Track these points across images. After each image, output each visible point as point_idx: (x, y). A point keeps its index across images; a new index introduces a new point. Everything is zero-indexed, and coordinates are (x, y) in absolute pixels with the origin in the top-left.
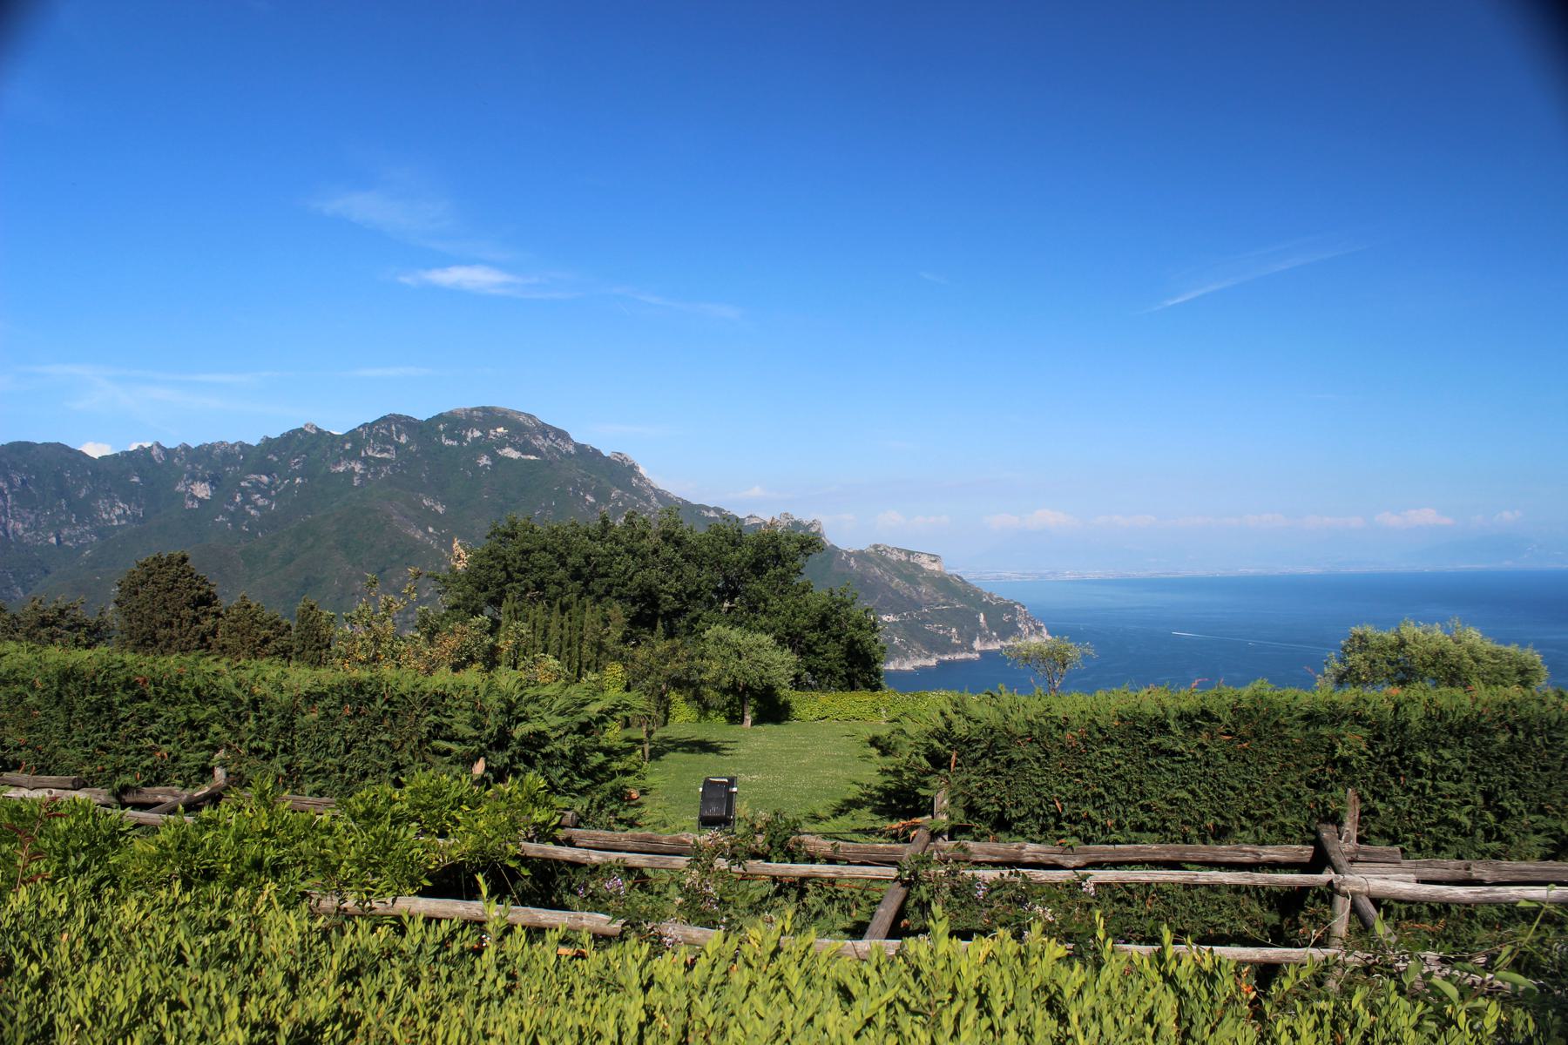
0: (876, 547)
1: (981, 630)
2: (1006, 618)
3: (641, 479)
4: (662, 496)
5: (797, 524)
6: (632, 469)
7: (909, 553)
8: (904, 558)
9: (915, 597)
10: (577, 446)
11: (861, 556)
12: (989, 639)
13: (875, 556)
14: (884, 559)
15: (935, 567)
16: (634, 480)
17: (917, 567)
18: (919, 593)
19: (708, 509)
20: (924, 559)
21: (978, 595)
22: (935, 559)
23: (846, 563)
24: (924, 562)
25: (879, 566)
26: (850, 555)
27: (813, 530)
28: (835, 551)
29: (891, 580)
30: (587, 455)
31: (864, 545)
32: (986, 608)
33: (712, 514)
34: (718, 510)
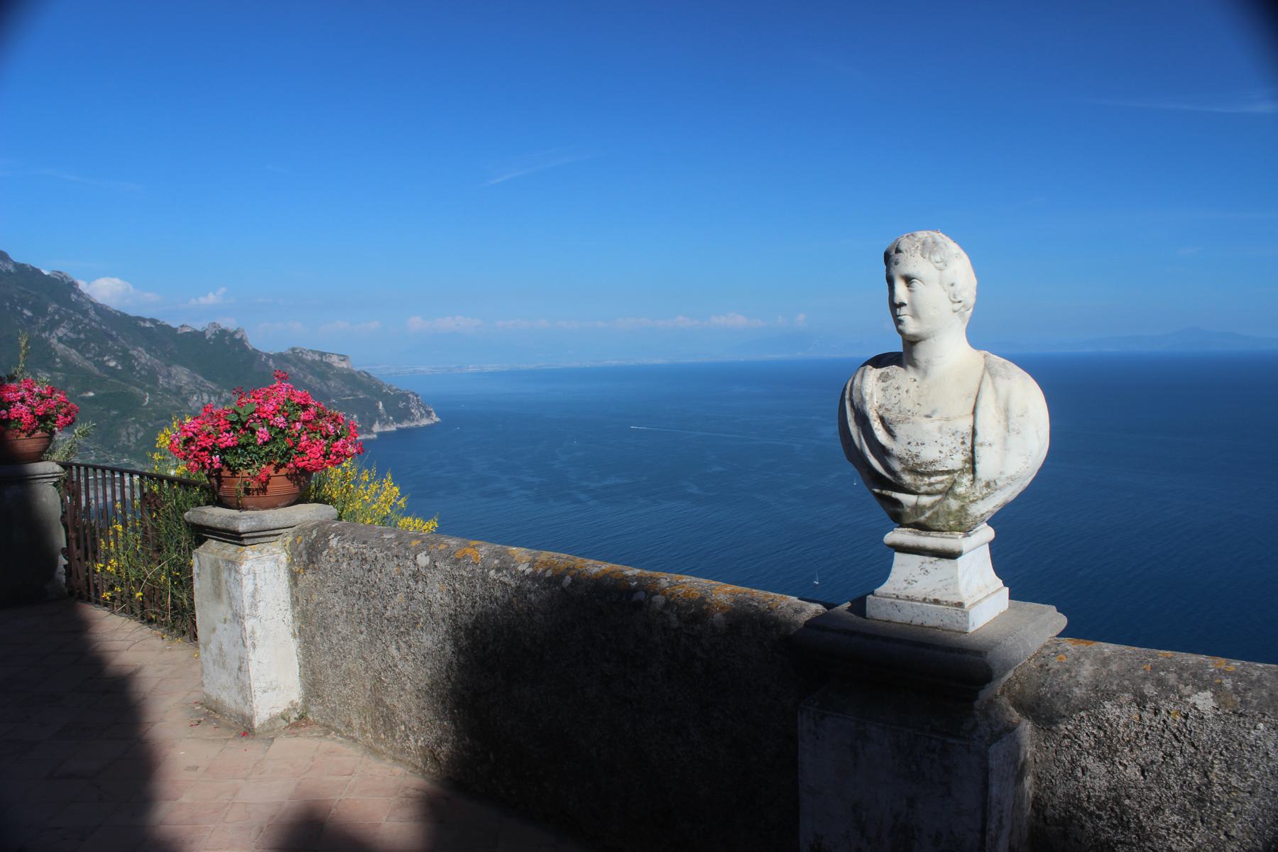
0: (293, 349)
1: (379, 416)
2: (401, 405)
3: (80, 294)
4: (101, 310)
5: (224, 332)
6: (72, 286)
7: (322, 354)
8: (317, 358)
9: (325, 388)
10: (16, 265)
11: (280, 358)
12: (387, 423)
13: (294, 357)
14: (301, 360)
15: (344, 365)
16: (73, 297)
17: (329, 365)
18: (328, 387)
19: (144, 320)
20: (335, 359)
21: (379, 387)
22: (344, 358)
23: (266, 364)
24: (334, 360)
25: (295, 365)
26: (269, 356)
27: (238, 337)
28: (255, 354)
29: (305, 377)
30: (28, 274)
31: (284, 349)
32: (385, 398)
33: (148, 325)
34: (153, 321)
